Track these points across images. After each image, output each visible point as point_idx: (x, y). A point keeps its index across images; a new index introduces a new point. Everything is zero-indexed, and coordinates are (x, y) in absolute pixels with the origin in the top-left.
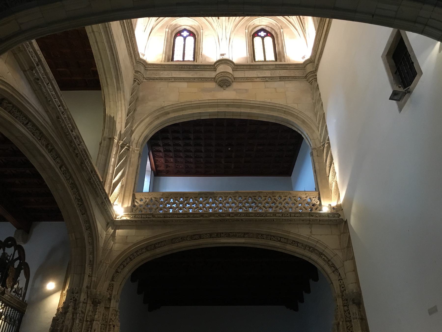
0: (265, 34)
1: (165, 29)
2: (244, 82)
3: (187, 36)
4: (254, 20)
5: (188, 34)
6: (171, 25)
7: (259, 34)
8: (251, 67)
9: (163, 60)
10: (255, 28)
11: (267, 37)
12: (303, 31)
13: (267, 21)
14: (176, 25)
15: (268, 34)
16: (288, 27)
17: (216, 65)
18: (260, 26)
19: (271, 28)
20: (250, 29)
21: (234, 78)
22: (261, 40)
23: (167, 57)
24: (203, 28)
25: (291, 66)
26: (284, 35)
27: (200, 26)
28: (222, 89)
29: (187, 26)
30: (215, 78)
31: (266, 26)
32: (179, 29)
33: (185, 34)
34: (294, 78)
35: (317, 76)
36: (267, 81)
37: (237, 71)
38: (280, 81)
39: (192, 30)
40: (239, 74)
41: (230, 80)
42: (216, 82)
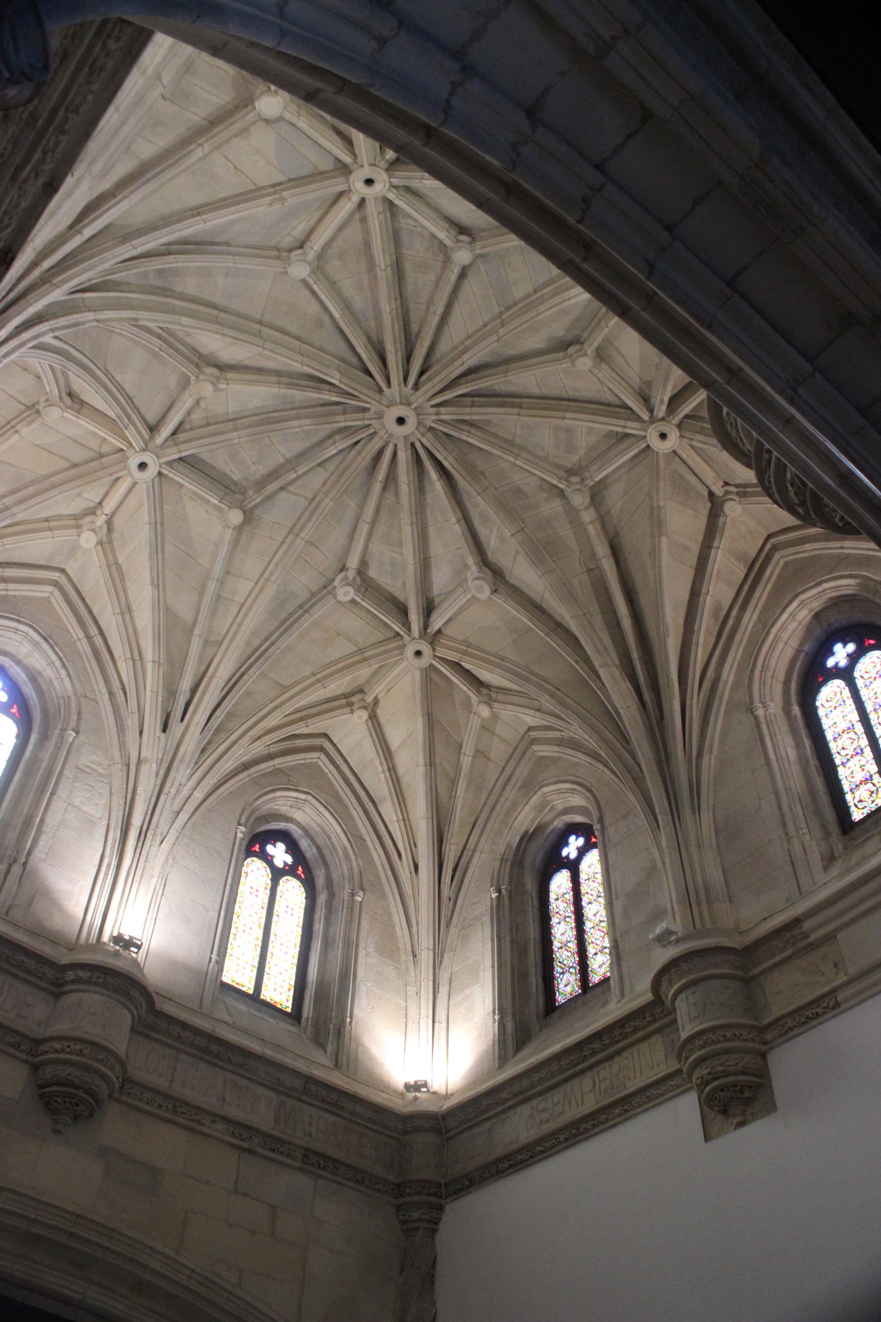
0: (289, 859)
2: (154, 1116)
4: (278, 794)
7: (270, 849)
8: (215, 1048)
13: (319, 820)
15: (302, 867)
16: (382, 895)
17: (70, 975)
19: (319, 849)
21: (126, 1080)
24: (83, 727)
25: (359, 1109)
26: (363, 923)
27: (74, 706)
29: (19, 663)
30: (38, 1042)
34: (357, 1177)
35: (445, 1217)
36: (251, 1152)
37: (148, 1037)
38: (301, 1169)
39: (28, 689)
40: (151, 1065)
41: (104, 1090)
42: (35, 1068)
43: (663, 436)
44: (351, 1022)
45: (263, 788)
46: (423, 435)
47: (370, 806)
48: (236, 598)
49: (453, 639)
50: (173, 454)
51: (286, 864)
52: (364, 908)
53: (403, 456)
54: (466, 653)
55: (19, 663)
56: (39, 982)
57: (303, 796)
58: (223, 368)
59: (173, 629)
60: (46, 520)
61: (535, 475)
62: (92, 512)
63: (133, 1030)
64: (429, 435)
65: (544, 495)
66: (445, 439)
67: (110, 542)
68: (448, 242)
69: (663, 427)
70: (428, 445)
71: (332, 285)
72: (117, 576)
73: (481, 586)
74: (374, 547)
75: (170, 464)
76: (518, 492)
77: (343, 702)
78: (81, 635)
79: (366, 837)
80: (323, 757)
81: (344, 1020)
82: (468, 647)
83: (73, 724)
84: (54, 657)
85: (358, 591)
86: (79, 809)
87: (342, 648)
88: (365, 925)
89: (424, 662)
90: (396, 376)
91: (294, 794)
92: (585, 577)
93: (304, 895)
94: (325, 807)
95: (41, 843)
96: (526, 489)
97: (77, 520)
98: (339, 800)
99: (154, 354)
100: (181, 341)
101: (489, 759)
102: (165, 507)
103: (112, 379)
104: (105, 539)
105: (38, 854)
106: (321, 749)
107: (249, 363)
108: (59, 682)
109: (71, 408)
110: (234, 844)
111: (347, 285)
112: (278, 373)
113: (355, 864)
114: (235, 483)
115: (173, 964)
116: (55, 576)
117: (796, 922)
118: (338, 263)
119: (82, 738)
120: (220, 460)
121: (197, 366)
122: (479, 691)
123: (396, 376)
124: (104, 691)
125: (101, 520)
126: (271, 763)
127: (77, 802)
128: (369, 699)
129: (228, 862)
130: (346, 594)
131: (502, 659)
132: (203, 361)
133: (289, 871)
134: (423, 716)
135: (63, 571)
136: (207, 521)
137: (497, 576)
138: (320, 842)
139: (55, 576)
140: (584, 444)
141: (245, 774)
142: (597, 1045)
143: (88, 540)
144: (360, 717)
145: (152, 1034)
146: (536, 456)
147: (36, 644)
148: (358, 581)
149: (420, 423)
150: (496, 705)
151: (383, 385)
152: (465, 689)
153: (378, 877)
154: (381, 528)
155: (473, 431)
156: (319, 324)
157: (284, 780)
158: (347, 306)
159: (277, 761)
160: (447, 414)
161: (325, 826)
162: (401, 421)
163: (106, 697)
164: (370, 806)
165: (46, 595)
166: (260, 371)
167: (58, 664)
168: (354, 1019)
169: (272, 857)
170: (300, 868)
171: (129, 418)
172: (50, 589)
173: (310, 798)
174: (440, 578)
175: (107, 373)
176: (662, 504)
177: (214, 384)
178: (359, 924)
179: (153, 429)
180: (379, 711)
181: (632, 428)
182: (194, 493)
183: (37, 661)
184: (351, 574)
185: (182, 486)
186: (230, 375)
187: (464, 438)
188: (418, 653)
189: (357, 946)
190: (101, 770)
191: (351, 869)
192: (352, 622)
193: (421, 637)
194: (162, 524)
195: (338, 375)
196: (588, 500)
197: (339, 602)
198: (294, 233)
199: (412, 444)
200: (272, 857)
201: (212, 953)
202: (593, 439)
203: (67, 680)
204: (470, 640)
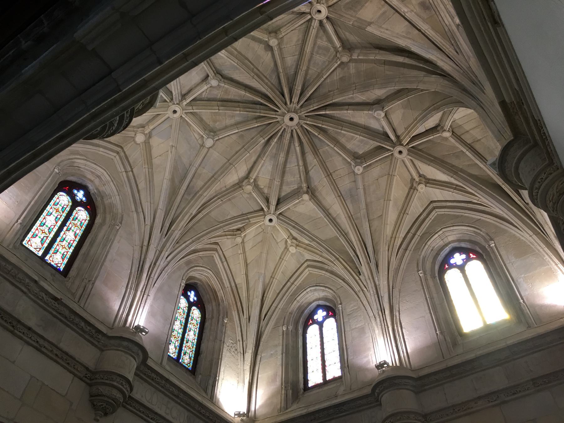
0: (464, 256)
1: (281, 328)
3: (325, 318)
4: (429, 243)
5: (325, 313)
6: (291, 313)
7: (452, 261)
9: (283, 405)
10: (438, 254)
11: (468, 263)
12: (536, 234)
14: (299, 307)
16: (505, 231)
18: (446, 245)
20: (428, 265)
22: (461, 275)
23: (290, 392)
31: (459, 241)
32: (307, 312)
33: (320, 315)
36: (504, 402)
37: (425, 390)
39: (328, 304)
43: (319, 11)
44: (524, 301)
45: (420, 248)
46: (301, 112)
47: (470, 206)
48: (338, 213)
49: (403, 133)
50: (273, 208)
51: (463, 260)
52: (498, 246)
54: (409, 132)
55: (319, 299)
56: (371, 405)
57: (441, 232)
58: (247, 177)
59: (330, 246)
60: (280, 258)
61: (336, 68)
62: (286, 242)
63: (417, 393)
64: (302, 109)
65: (346, 68)
66: (309, 101)
67: (300, 242)
68: (209, 86)
69: (314, 11)
70: (305, 112)
71: (226, 128)
72: (308, 248)
74: (349, 146)
75: (276, 209)
76: (342, 79)
77: (412, 190)
78: (324, 272)
79: (479, 217)
80: (437, 210)
81: (520, 303)
82: (408, 129)
83: (339, 302)
84: (322, 288)
85: (360, 164)
86: (356, 328)
87: (383, 181)
88: (503, 253)
89: (405, 152)
91: (437, 235)
92: (386, 67)
93: (459, 271)
94: (453, 226)
95: (349, 353)
96: (341, 76)
97: (286, 248)
98: (457, 217)
99: (230, 200)
100: (227, 190)
101: (480, 140)
102: (292, 219)
103: (226, 221)
104: (298, 243)
105: (350, 358)
106: (434, 208)
107: (250, 166)
108: (328, 293)
109: (242, 232)
110: (421, 281)
111: (229, 122)
112: (259, 157)
113: (481, 233)
114: (298, 189)
115: (421, 351)
116: (306, 264)
117: (503, 104)
118: (218, 123)
119: (343, 303)
120: (286, 190)
121: (240, 187)
122: (438, 131)
124: (341, 281)
125: (289, 242)
126: (416, 236)
127: (354, 327)
128: (417, 179)
129: (422, 290)
130: (359, 170)
131: (416, 118)
132: (239, 185)
133: (468, 259)
134: (429, 165)
135: (307, 260)
136: (304, 207)
137: (378, 103)
138: (467, 238)
139: (306, 264)
140: (326, 43)
141: (408, 252)
143: (292, 250)
144: (422, 188)
145: (425, 387)
146: (328, 65)
147: (315, 290)
148: (359, 161)
149: (295, 112)
150: (445, 128)
152: (432, 137)
153: (496, 227)
154: (343, 140)
155: (308, 89)
156: (242, 137)
157: (428, 235)
158: (237, 124)
159: (418, 233)
160: (295, 100)
161: (460, 232)
162: (291, 119)
163: (343, 282)
164: (470, 206)
165: (308, 273)
166: (255, 163)
167: (324, 288)
168: (524, 298)
169: (455, 263)
170: (471, 255)
171: (248, 219)
172: (307, 270)
173: (444, 230)
174: (374, 125)
175: (222, 222)
176: (351, 23)
177: (249, 184)
178: (500, 255)
179: (262, 209)
180: (428, 177)
181: (315, 24)
182: (294, 205)
183: (322, 294)
184: (353, 164)
185: (289, 208)
186: (251, 175)
187: (308, 95)
188: (400, 152)
189: (505, 265)
190: (356, 308)
191: (483, 237)
192: (376, 171)
193: (394, 148)
194: (297, 223)
195: (262, 138)
197: (362, 173)
198: (198, 138)
199: (306, 116)
200: (455, 263)
201: (436, 331)
202: (325, 38)
203: (329, 290)
204: (406, 127)
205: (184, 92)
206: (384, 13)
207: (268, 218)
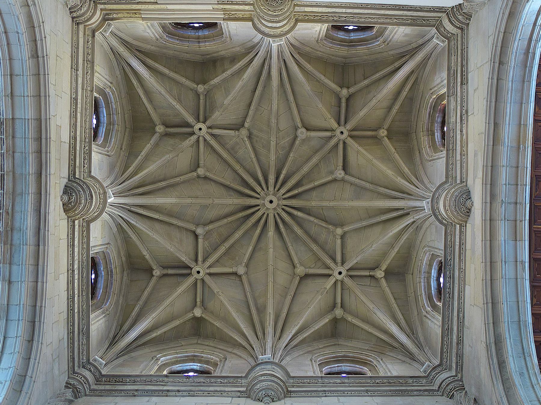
28: (473, 209)
43: (200, 129)
50: (332, 265)
53: (283, 191)
73: (301, 133)
90: (259, 214)
123: (259, 214)
142: (335, 19)
151: (265, 216)
160: (258, 189)
196: (241, 130)
199: (278, 191)
205: (194, 258)
206: (225, 89)
207: (336, 273)
